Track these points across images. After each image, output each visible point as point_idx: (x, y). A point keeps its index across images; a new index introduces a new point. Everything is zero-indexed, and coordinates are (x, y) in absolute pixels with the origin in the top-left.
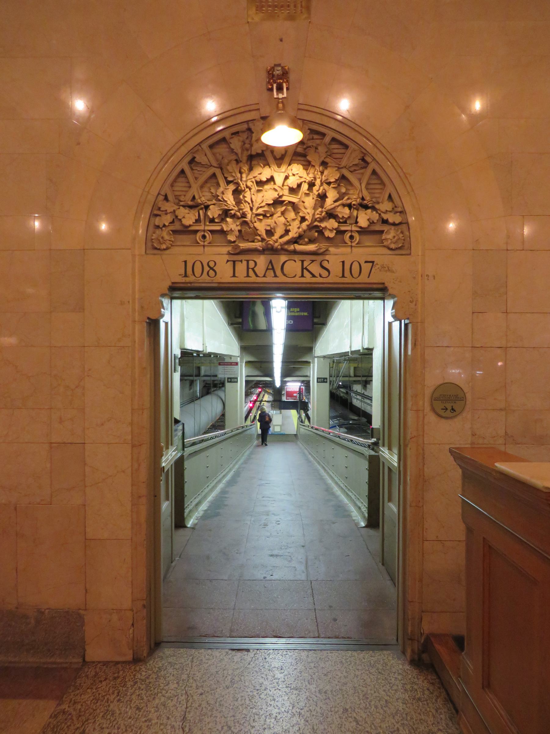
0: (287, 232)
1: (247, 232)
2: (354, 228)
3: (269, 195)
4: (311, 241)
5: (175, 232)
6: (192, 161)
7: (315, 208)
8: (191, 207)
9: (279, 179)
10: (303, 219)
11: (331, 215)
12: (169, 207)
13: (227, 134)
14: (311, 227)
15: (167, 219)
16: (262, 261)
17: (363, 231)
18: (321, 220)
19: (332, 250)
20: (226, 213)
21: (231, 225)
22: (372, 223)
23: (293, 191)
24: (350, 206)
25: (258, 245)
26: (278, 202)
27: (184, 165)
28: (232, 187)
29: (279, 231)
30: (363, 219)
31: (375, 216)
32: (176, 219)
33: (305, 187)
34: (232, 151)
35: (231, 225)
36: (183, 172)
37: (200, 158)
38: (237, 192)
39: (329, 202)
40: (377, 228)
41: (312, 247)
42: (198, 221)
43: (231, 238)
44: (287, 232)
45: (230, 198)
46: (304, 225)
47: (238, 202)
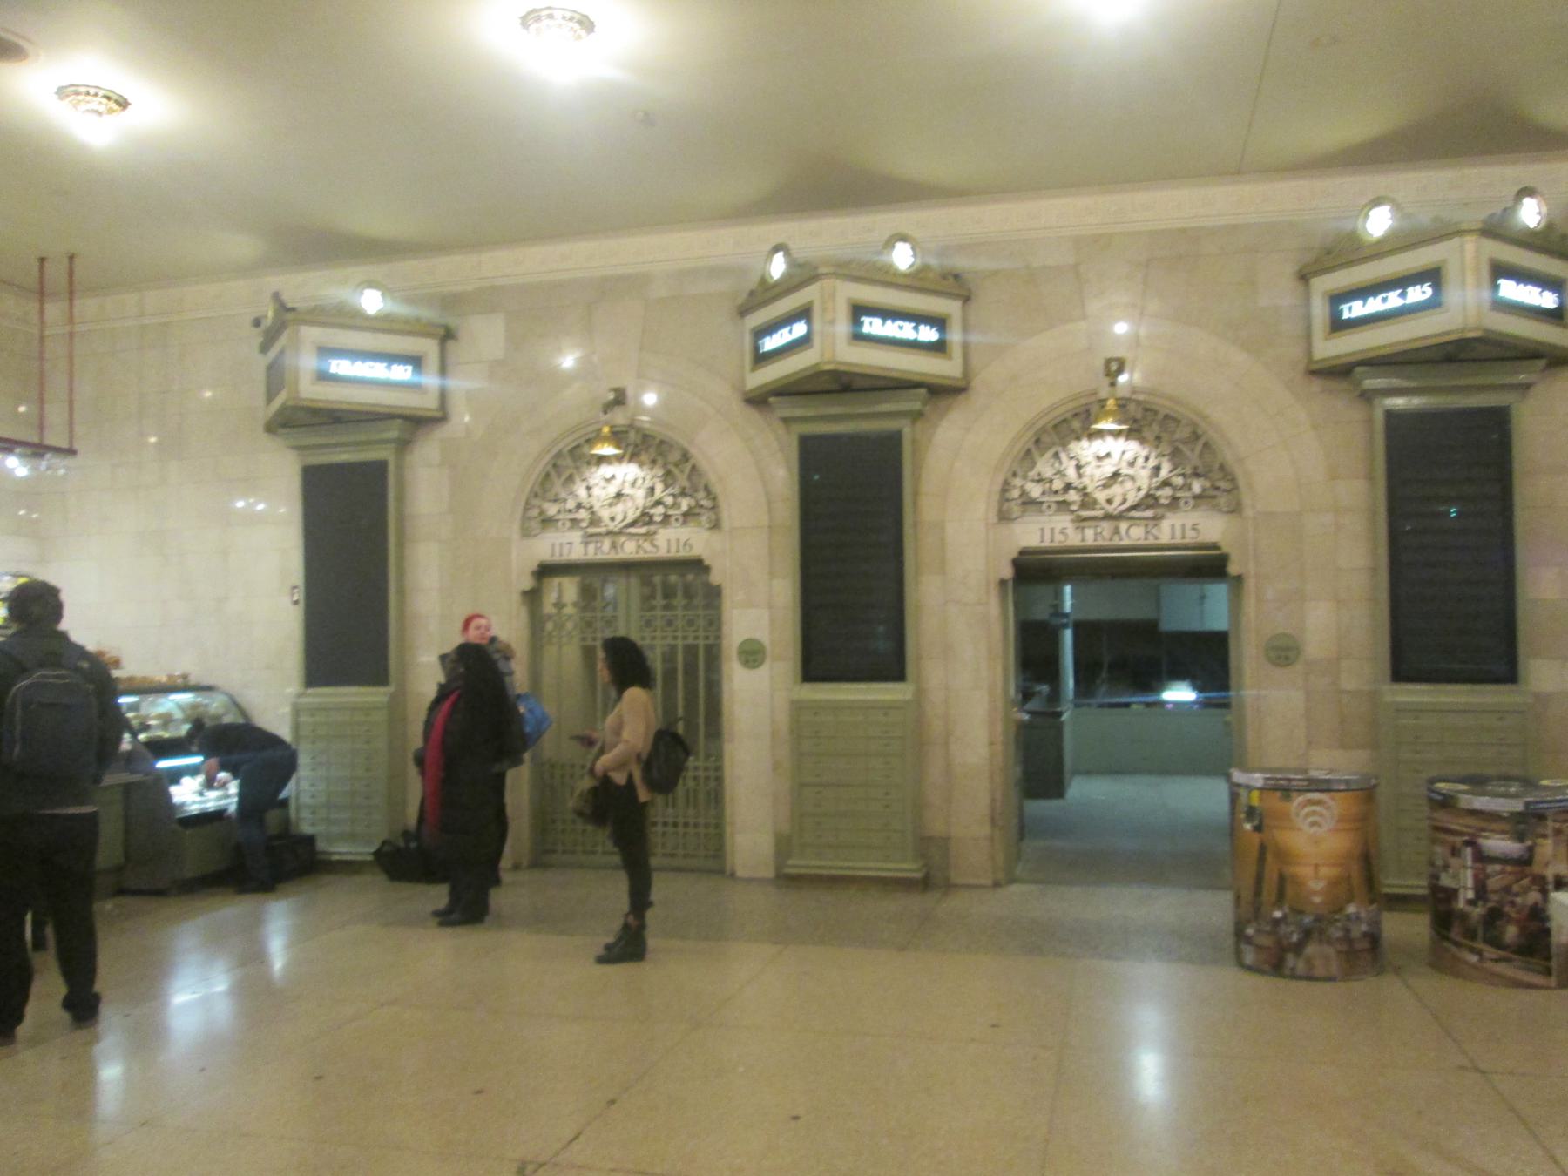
0: (1125, 501)
1: (1088, 502)
2: (1187, 494)
3: (1108, 468)
4: (1148, 507)
5: (1024, 503)
6: (1037, 441)
7: (1151, 477)
8: (1039, 481)
9: (1116, 456)
10: (1139, 489)
11: (1166, 483)
12: (1018, 482)
13: (1068, 415)
14: (1148, 496)
15: (1016, 493)
16: (1106, 527)
17: (1196, 497)
18: (1158, 488)
19: (1169, 514)
20: (1068, 487)
21: (1073, 496)
22: (1204, 490)
23: (1132, 464)
24: (1183, 475)
25: (1099, 513)
26: (1116, 475)
27: (1031, 445)
28: (1073, 463)
29: (1117, 501)
30: (1197, 487)
31: (1208, 484)
32: (1024, 493)
33: (1140, 461)
34: (1073, 431)
35: (1073, 496)
36: (1028, 452)
37: (1046, 439)
38: (1078, 467)
39: (1164, 473)
40: (1212, 493)
41: (1149, 513)
42: (1043, 493)
43: (1074, 507)
44: (1125, 501)
45: (1071, 473)
46: (1142, 493)
47: (1080, 476)
